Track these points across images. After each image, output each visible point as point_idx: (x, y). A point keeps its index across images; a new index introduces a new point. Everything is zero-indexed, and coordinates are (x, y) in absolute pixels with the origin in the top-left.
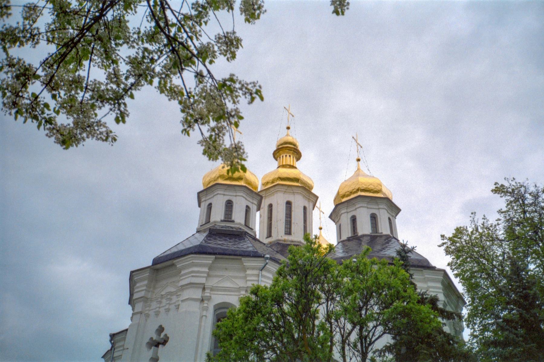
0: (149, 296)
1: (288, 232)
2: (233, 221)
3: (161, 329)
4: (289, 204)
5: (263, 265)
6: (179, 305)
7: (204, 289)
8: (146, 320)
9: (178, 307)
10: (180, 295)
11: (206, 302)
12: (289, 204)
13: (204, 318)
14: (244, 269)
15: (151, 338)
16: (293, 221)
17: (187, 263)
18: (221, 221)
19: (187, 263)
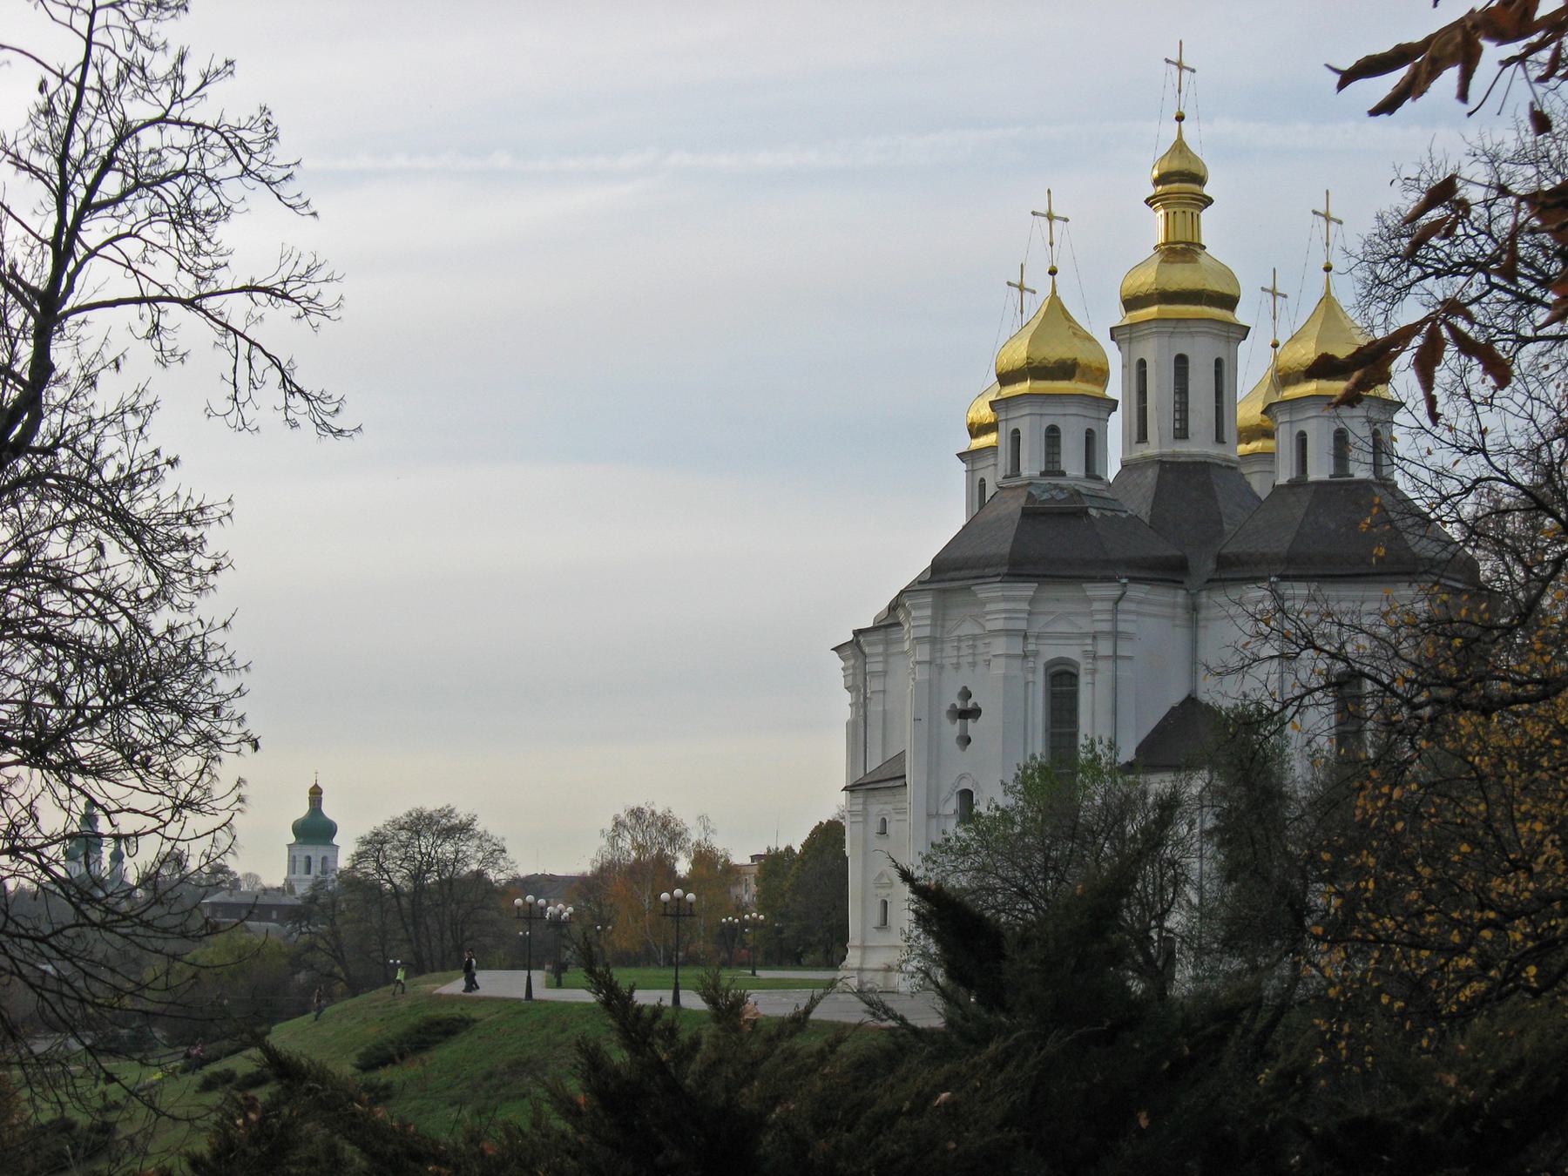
2: (1063, 474)
3: (966, 694)
4: (1181, 362)
5: (1119, 593)
6: (989, 661)
7: (1025, 637)
8: (940, 674)
10: (989, 643)
11: (1031, 659)
12: (1181, 362)
13: (1031, 684)
14: (1090, 600)
15: (954, 705)
16: (1190, 406)
17: (992, 594)
18: (1043, 474)
19: (992, 594)
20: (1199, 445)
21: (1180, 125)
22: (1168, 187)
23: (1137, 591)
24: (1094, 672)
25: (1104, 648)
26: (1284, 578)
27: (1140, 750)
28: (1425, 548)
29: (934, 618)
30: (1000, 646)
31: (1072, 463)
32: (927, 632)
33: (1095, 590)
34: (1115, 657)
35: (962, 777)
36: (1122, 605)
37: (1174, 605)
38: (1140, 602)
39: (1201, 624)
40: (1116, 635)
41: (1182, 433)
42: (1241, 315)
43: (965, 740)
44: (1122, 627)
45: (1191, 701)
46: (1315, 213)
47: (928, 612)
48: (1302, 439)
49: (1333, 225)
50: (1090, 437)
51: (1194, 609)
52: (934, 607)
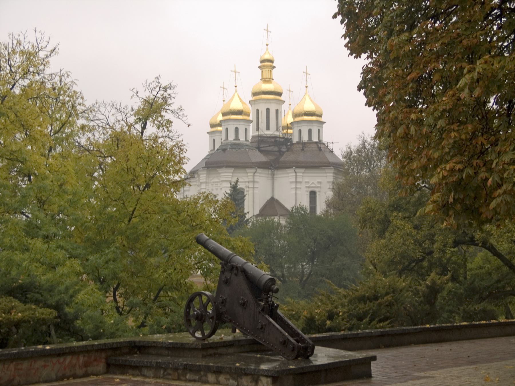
0: (207, 181)
1: (268, 128)
2: (239, 140)
4: (268, 110)
5: (255, 171)
9: (221, 189)
12: (268, 110)
14: (247, 173)
18: (234, 140)
20: (272, 132)
21: (267, 48)
22: (263, 64)
23: (259, 170)
24: (248, 191)
25: (251, 185)
28: (331, 160)
29: (206, 177)
31: (242, 138)
32: (204, 180)
33: (248, 170)
34: (254, 188)
36: (255, 174)
37: (268, 174)
38: (260, 173)
39: (275, 179)
40: (254, 182)
41: (268, 128)
42: (282, 98)
44: (255, 180)
46: (304, 72)
47: (205, 175)
48: (300, 131)
49: (308, 75)
50: (246, 130)
51: (273, 175)
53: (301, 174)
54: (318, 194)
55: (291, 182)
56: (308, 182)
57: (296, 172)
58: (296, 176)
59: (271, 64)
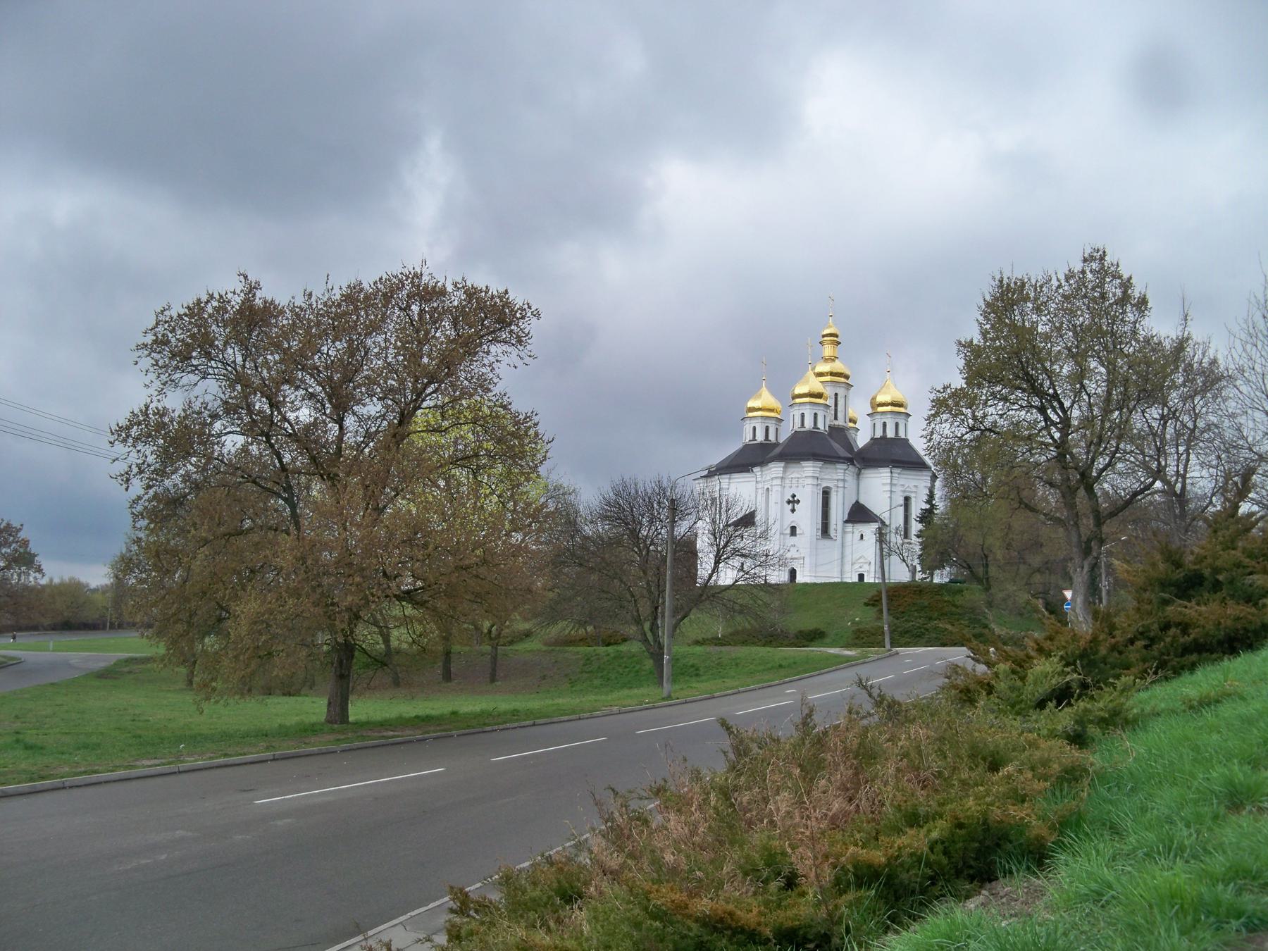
3: (794, 496)
9: (804, 487)
12: (836, 394)
14: (837, 469)
20: (840, 422)
25: (841, 484)
26: (893, 466)
27: (849, 514)
30: (809, 481)
32: (781, 475)
33: (839, 466)
35: (792, 522)
40: (844, 481)
43: (793, 511)
45: (857, 502)
48: (885, 425)
52: (783, 468)
53: (897, 475)
54: (913, 500)
55: (884, 484)
56: (903, 485)
57: (891, 472)
58: (892, 477)
59: (835, 339)
